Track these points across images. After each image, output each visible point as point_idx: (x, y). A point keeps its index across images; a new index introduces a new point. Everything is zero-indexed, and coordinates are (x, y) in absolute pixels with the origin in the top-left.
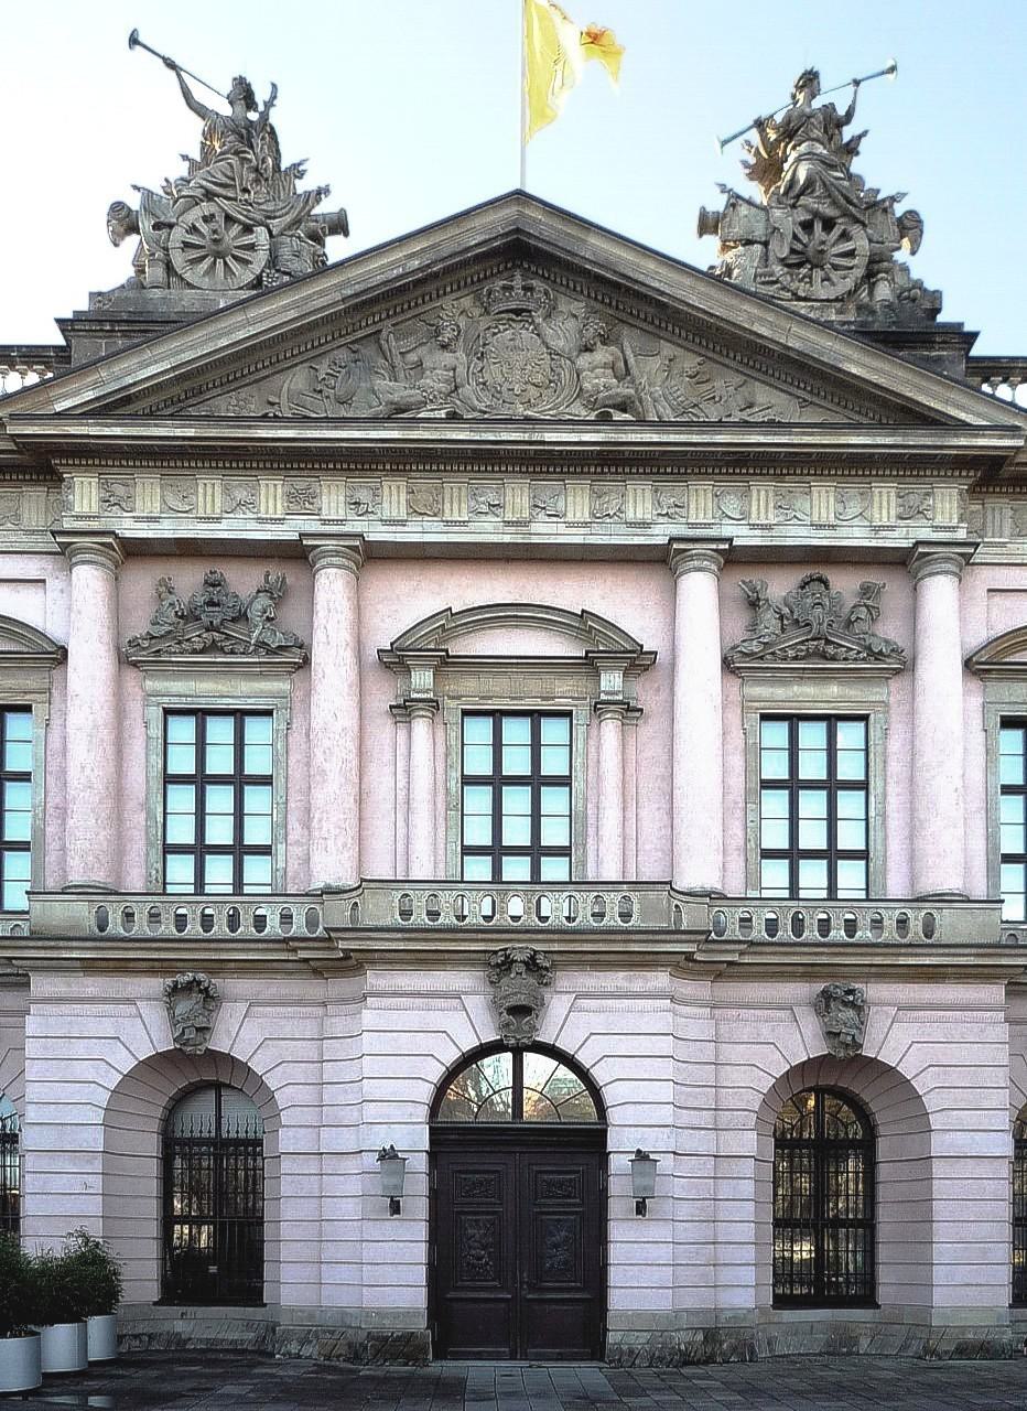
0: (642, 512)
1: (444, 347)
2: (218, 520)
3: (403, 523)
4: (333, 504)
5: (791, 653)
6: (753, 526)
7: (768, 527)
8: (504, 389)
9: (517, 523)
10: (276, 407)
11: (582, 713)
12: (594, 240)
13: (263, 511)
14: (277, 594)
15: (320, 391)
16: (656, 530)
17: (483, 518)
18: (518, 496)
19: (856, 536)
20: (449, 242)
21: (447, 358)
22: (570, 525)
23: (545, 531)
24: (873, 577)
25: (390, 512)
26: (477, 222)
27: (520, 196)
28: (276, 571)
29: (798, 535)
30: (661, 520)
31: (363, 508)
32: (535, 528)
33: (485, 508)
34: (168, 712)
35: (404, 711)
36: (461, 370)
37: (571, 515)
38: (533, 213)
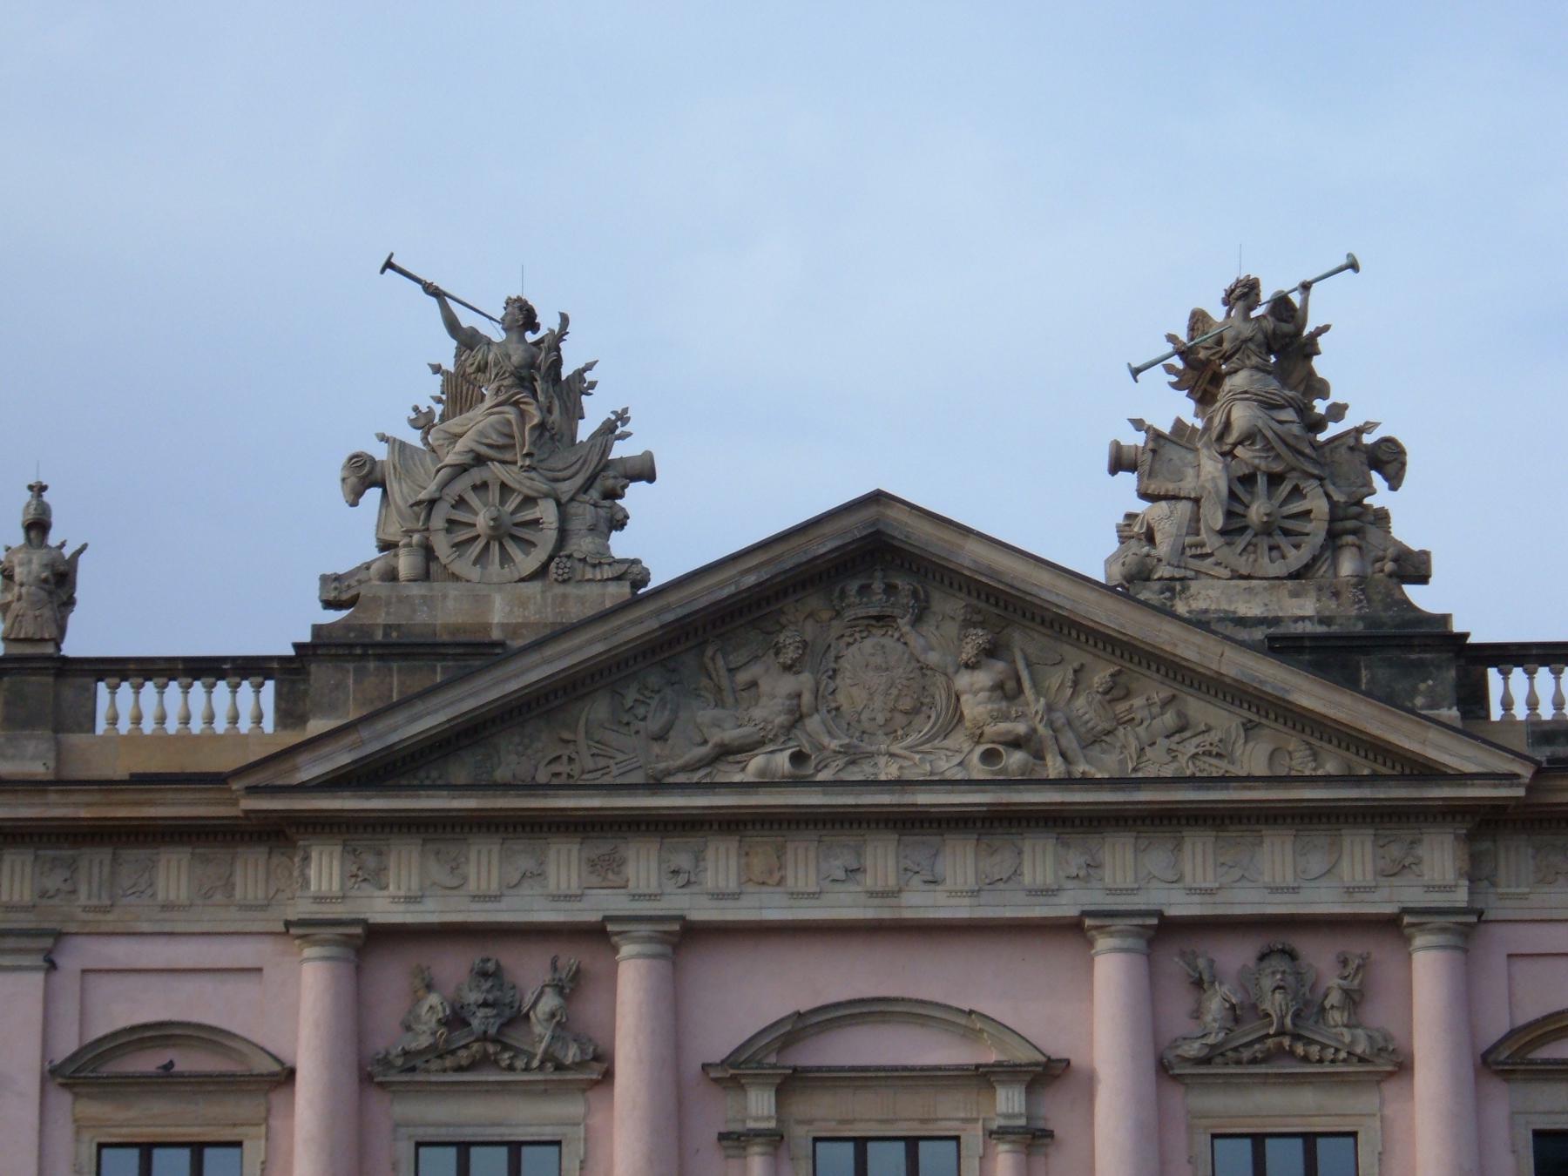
0: (1043, 876)
1: (788, 668)
2: (496, 898)
3: (736, 896)
4: (645, 879)
5: (1246, 1054)
6: (1191, 891)
7: (1209, 892)
8: (864, 717)
9: (884, 894)
10: (571, 746)
11: (973, 1138)
12: (972, 546)
13: (557, 886)
14: (570, 987)
15: (628, 724)
16: (1064, 898)
17: (838, 887)
18: (882, 859)
19: (1324, 901)
20: (792, 558)
21: (788, 684)
22: (952, 893)
23: (921, 904)
24: (1356, 946)
25: (719, 884)
26: (827, 529)
27: (878, 498)
28: (572, 956)
29: (1247, 901)
30: (1070, 884)
31: (682, 879)
32: (908, 898)
33: (841, 875)
34: (419, 1145)
35: (735, 1141)
36: (807, 698)
37: (955, 882)
38: (893, 513)
